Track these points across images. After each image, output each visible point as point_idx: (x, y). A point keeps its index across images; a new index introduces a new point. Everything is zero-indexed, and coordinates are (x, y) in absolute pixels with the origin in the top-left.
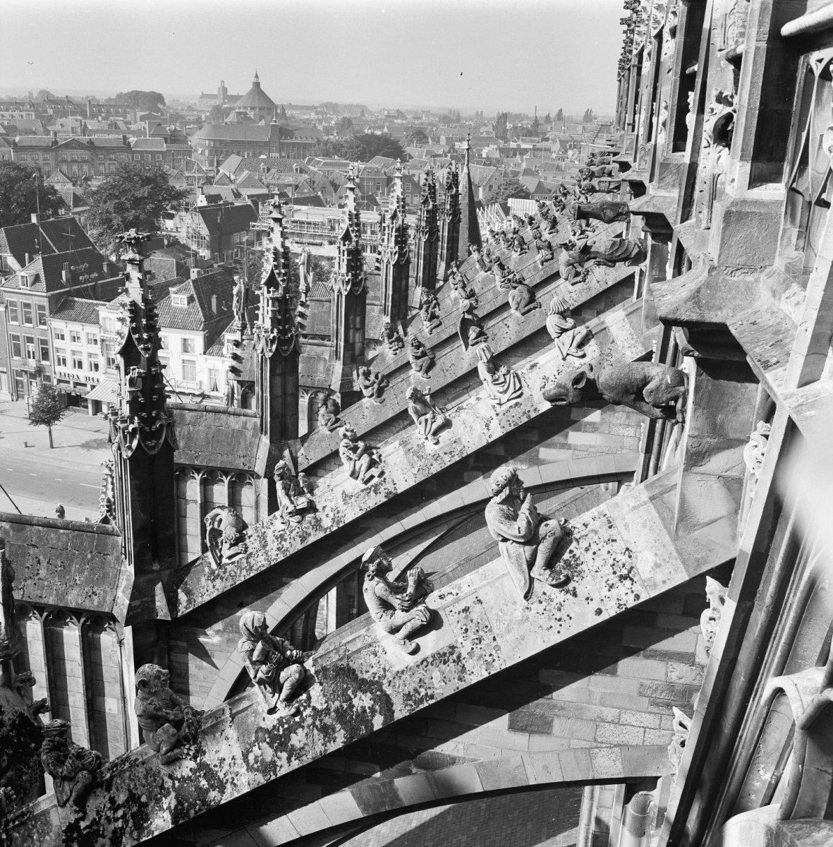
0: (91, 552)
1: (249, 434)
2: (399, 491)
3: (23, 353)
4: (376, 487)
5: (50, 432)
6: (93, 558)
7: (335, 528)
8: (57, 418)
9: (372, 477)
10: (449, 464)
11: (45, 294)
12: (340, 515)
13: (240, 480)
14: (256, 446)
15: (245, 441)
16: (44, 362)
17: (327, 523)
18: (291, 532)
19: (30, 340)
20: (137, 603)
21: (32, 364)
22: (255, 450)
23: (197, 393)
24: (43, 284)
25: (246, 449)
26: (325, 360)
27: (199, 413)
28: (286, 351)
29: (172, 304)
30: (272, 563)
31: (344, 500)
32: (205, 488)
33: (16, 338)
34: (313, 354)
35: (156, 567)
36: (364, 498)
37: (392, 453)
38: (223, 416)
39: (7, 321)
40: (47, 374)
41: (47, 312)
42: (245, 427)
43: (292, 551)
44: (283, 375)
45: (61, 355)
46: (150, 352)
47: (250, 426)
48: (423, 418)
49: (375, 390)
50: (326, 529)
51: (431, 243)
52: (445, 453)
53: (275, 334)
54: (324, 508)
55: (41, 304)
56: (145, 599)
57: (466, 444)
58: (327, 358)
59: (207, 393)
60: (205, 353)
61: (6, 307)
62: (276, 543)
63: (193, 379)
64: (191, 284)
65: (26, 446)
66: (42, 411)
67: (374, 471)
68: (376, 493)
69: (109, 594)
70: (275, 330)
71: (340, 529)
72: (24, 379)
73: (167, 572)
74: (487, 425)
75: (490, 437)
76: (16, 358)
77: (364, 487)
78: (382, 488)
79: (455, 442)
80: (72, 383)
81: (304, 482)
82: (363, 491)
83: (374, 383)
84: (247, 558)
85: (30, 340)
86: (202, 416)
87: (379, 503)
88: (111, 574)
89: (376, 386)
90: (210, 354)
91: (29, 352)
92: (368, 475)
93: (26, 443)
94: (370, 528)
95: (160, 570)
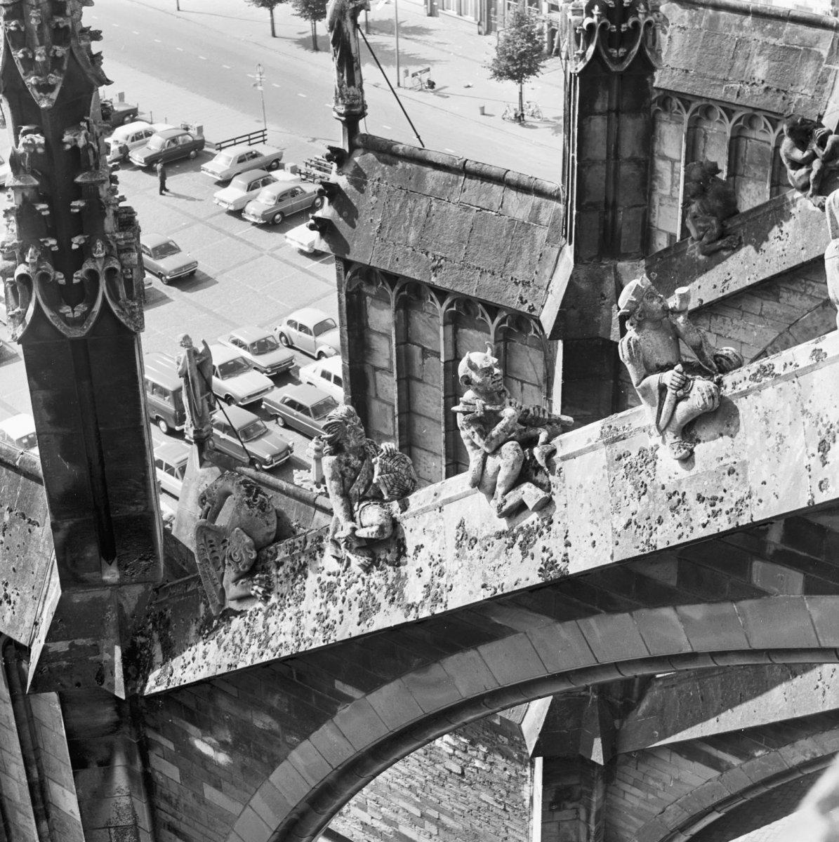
0: (10, 510)
1: (542, 234)
2: (573, 569)
4: (529, 533)
5: (521, 93)
6: (12, 522)
7: (425, 613)
8: (531, 71)
9: (521, 507)
10: (700, 533)
12: (443, 581)
13: (520, 328)
14: (551, 264)
15: (532, 249)
17: (414, 591)
18: (349, 586)
20: (62, 646)
22: (548, 272)
25: (531, 266)
26: (819, 57)
27: (453, 177)
28: (622, 59)
30: (302, 649)
31: (459, 546)
32: (455, 332)
34: (796, 40)
35: (111, 575)
36: (498, 556)
37: (581, 453)
38: (497, 189)
42: (535, 217)
43: (340, 634)
44: (614, 113)
46: (54, 96)
47: (545, 216)
48: (653, 380)
49: (812, 176)
50: (410, 606)
52: (700, 498)
53: (595, 20)
54: (419, 548)
56: (80, 642)
57: (756, 486)
58: (825, 54)
62: (319, 601)
65: (484, 114)
66: (510, 58)
67: (530, 493)
68: (525, 554)
69: (30, 608)
70: (596, 10)
71: (434, 618)
73: (138, 590)
74: (824, 447)
75: (822, 486)
77: (503, 524)
78: (540, 543)
79: (731, 472)
81: (384, 469)
82: (499, 535)
83: (814, 156)
84: (267, 615)
86: (456, 182)
87: (524, 584)
88: (37, 567)
89: (816, 165)
92: (512, 499)
93: (483, 109)
94: (514, 632)
95: (120, 584)
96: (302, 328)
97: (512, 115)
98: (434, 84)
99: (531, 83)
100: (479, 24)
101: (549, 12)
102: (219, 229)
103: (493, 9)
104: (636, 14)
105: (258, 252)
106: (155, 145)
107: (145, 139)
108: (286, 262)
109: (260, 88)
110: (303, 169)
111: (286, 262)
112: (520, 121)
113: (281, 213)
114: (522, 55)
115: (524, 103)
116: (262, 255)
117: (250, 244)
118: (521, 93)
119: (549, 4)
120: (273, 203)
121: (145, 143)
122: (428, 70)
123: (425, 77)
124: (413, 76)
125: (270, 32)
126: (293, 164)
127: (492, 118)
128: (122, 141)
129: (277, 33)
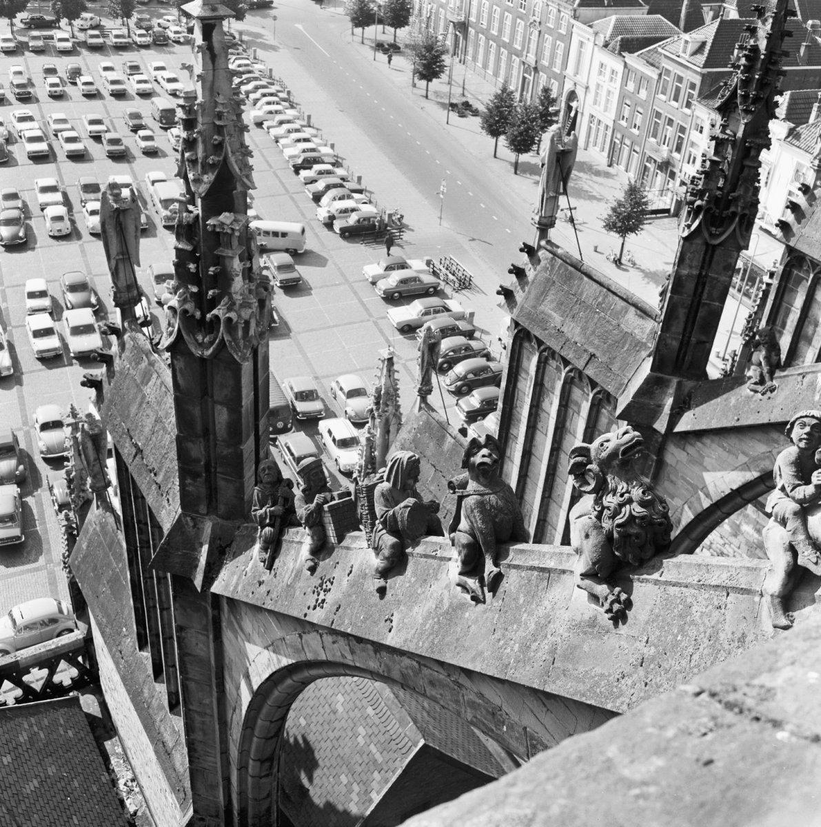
3: (659, 135)
5: (623, 244)
8: (633, 229)
11: (699, 70)
16: (675, 155)
19: (670, 122)
21: (664, 152)
24: (701, 59)
33: (658, 115)
40: (675, 170)
41: (696, 93)
45: (694, 151)
51: (710, 250)
55: (694, 81)
61: (660, 75)
65: (596, 251)
72: (651, 166)
76: (652, 140)
85: (670, 122)
91: (666, 136)
93: (596, 247)
96: (341, 389)
97: (612, 257)
99: (631, 237)
101: (680, 186)
102: (355, 293)
103: (647, 173)
104: (737, 206)
105: (367, 317)
106: (352, 220)
107: (350, 213)
108: (381, 331)
109: (442, 196)
110: (437, 263)
111: (381, 331)
112: (616, 264)
113: (399, 292)
114: (629, 217)
115: (625, 251)
116: (368, 320)
117: (367, 310)
118: (623, 244)
119: (681, 181)
120: (395, 284)
121: (347, 217)
125: (493, 153)
126: (429, 258)
127: (600, 255)
128: (333, 211)
129: (497, 156)
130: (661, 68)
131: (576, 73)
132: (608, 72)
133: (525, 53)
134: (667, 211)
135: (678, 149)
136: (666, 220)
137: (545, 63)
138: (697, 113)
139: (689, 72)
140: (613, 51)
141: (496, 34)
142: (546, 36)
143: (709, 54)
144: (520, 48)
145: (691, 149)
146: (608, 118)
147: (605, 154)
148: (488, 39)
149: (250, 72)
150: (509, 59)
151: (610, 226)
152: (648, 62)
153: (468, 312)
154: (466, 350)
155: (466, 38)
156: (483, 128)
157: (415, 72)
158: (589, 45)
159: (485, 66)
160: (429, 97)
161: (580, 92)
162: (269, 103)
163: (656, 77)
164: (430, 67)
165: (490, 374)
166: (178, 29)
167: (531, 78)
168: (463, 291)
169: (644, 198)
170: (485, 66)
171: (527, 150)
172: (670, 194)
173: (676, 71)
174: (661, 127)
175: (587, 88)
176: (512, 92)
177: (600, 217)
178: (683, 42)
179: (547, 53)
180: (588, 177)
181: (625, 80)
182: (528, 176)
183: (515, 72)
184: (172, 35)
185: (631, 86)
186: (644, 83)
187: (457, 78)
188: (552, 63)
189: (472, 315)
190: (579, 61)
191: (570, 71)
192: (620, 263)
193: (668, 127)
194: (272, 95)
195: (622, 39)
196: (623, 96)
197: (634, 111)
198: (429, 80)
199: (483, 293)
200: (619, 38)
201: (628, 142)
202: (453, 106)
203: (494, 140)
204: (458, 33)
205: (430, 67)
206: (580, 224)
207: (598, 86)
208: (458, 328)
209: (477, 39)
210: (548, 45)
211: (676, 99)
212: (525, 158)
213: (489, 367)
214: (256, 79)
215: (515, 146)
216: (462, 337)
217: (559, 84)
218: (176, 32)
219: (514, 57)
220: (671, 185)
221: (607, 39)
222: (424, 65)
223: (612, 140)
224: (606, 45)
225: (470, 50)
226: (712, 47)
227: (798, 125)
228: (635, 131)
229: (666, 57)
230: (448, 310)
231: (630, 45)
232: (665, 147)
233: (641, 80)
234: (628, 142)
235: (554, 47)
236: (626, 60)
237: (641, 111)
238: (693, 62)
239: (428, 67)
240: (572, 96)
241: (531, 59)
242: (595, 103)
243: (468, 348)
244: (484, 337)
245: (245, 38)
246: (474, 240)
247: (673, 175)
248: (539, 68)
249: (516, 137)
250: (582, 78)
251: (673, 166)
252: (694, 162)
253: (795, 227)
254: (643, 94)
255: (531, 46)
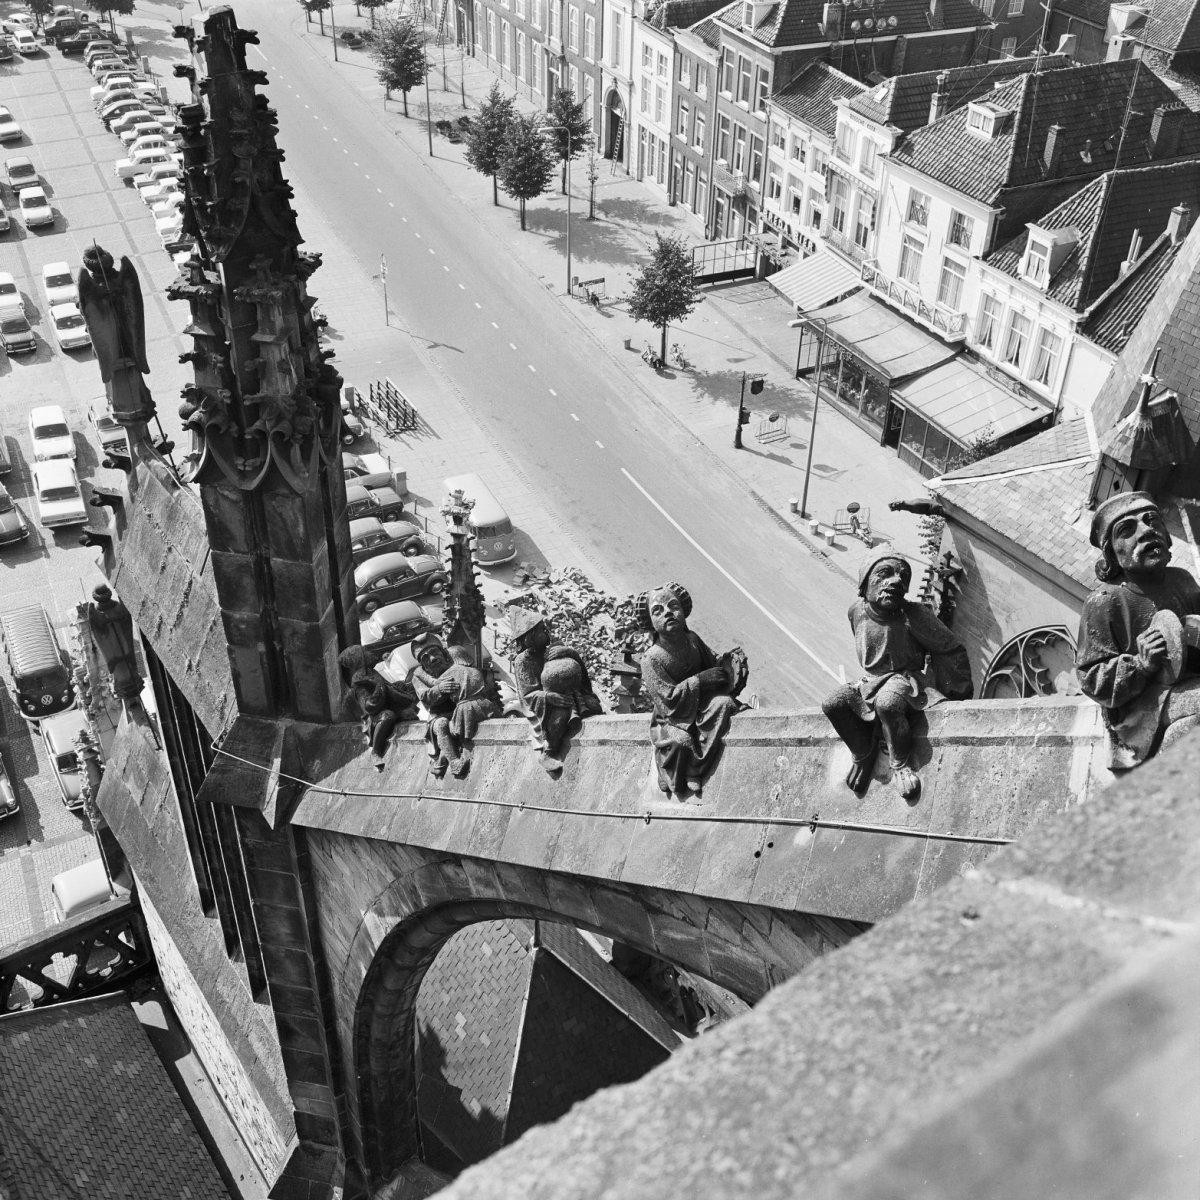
3: (730, 155)
5: (664, 335)
11: (767, 49)
16: (755, 185)
23: (949, 339)
24: (772, 32)
29: (967, 125)
33: (725, 123)
39: (719, 89)
41: (769, 86)
55: (765, 67)
59: (971, 342)
60: (985, 257)
63: (955, 304)
64: (1023, 86)
65: (628, 348)
80: (780, 236)
90: (995, 264)
98: (597, 299)
99: (674, 323)
100: (707, 227)
112: (655, 367)
118: (664, 335)
122: (603, 280)
123: (592, 289)
124: (581, 285)
127: (634, 355)
130: (721, 48)
131: (616, 64)
132: (655, 59)
133: (546, 36)
134: (751, 272)
135: (757, 176)
136: (749, 287)
137: (575, 49)
138: (774, 118)
139: (758, 55)
140: (658, 24)
141: (508, 8)
142: (571, 7)
143: (783, 23)
144: (539, 28)
145: (773, 175)
146: (662, 130)
147: (665, 186)
148: (499, 16)
149: (127, 96)
150: (530, 49)
151: (640, 310)
152: (706, 41)
153: (396, 470)
154: (380, 537)
155: (472, 17)
156: (470, 161)
157: (385, 77)
158: (627, 19)
159: (501, 59)
160: (411, 114)
161: (623, 92)
162: (147, 146)
163: (715, 63)
164: (405, 69)
165: (411, 579)
166: (29, 33)
167: (559, 73)
168: (402, 435)
169: (686, 262)
170: (501, 59)
171: (535, 193)
172: (753, 247)
173: (740, 53)
174: (730, 141)
175: (631, 85)
176: (509, 103)
177: (624, 296)
178: (744, 6)
179: (575, 33)
180: (634, 226)
181: (678, 69)
182: (542, 231)
183: (538, 67)
184: (19, 45)
185: (686, 81)
186: (703, 74)
187: (455, 78)
188: (583, 49)
189: (402, 476)
190: (617, 43)
191: (607, 61)
192: (666, 366)
193: (740, 141)
194: (156, 131)
195: (669, 6)
196: (678, 97)
197: (694, 118)
198: (406, 89)
199: (435, 435)
200: (665, 5)
201: (691, 166)
202: (444, 126)
203: (492, 177)
204: (461, 9)
205: (405, 69)
206: (609, 305)
207: (645, 81)
208: (373, 503)
209: (487, 17)
210: (575, 20)
211: (745, 97)
212: (533, 204)
213: (408, 567)
214: (136, 107)
215: (515, 186)
216: (373, 520)
217: (596, 82)
218: (24, 40)
219: (535, 42)
220: (753, 231)
221: (650, 7)
222: (393, 66)
223: (671, 165)
224: (648, 19)
225: (479, 34)
226: (787, 12)
227: (908, 129)
228: (699, 150)
229: (726, 32)
230: (362, 473)
231: (678, 18)
232: (739, 173)
233: (699, 67)
234: (691, 166)
235: (583, 24)
236: (677, 38)
237: (703, 117)
238: (761, 38)
239: (398, 67)
240: (614, 99)
241: (556, 46)
242: (644, 108)
243: (384, 536)
244: (422, 512)
245: (137, 40)
246: (436, 345)
247: (753, 215)
248: (567, 58)
249: (515, 173)
250: (623, 72)
251: (753, 203)
252: (778, 195)
253: (116, 544)
254: (703, 92)
255: (554, 24)
